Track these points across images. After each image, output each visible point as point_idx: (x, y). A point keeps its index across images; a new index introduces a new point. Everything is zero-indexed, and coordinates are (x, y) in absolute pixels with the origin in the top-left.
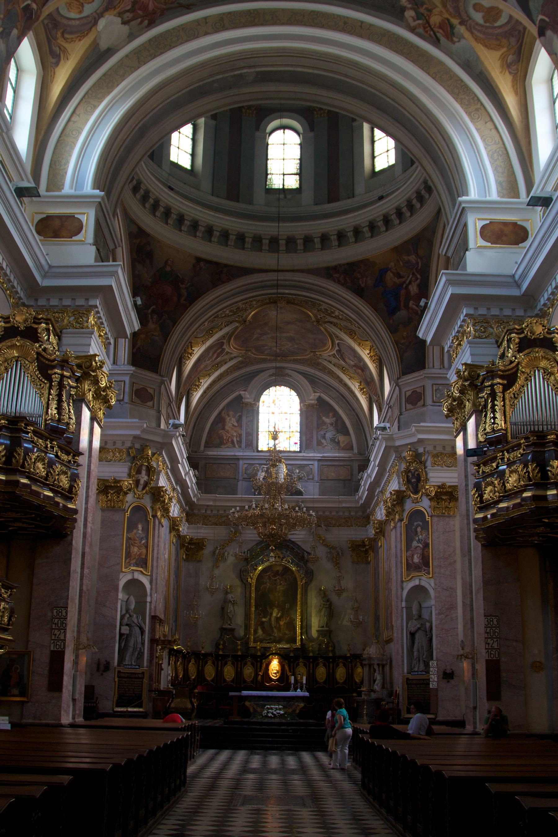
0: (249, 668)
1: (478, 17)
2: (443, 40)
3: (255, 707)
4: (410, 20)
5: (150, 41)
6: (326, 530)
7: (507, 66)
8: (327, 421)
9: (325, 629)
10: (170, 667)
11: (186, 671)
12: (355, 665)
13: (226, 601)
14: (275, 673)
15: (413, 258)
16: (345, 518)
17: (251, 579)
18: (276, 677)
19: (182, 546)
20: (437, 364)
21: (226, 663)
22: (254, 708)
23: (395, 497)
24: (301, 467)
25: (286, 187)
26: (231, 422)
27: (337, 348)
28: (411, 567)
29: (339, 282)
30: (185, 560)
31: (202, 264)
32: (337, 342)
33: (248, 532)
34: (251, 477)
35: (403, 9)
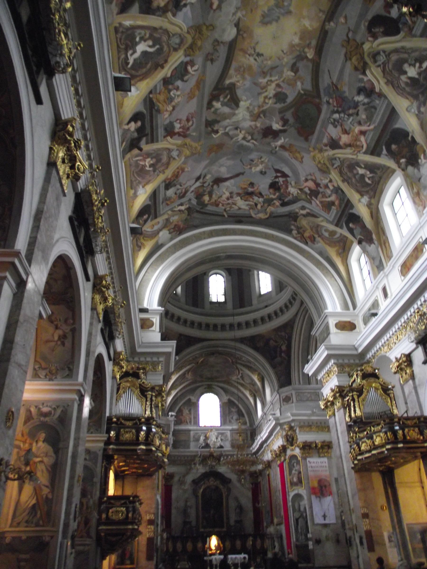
1: (326, 234)
2: (309, 243)
4: (295, 235)
5: (180, 241)
7: (339, 254)
8: (234, 410)
15: (283, 334)
20: (297, 382)
23: (281, 448)
24: (222, 434)
25: (219, 301)
26: (186, 411)
27: (241, 375)
28: (292, 484)
29: (247, 345)
31: (182, 337)
32: (241, 372)
34: (198, 440)
35: (292, 230)
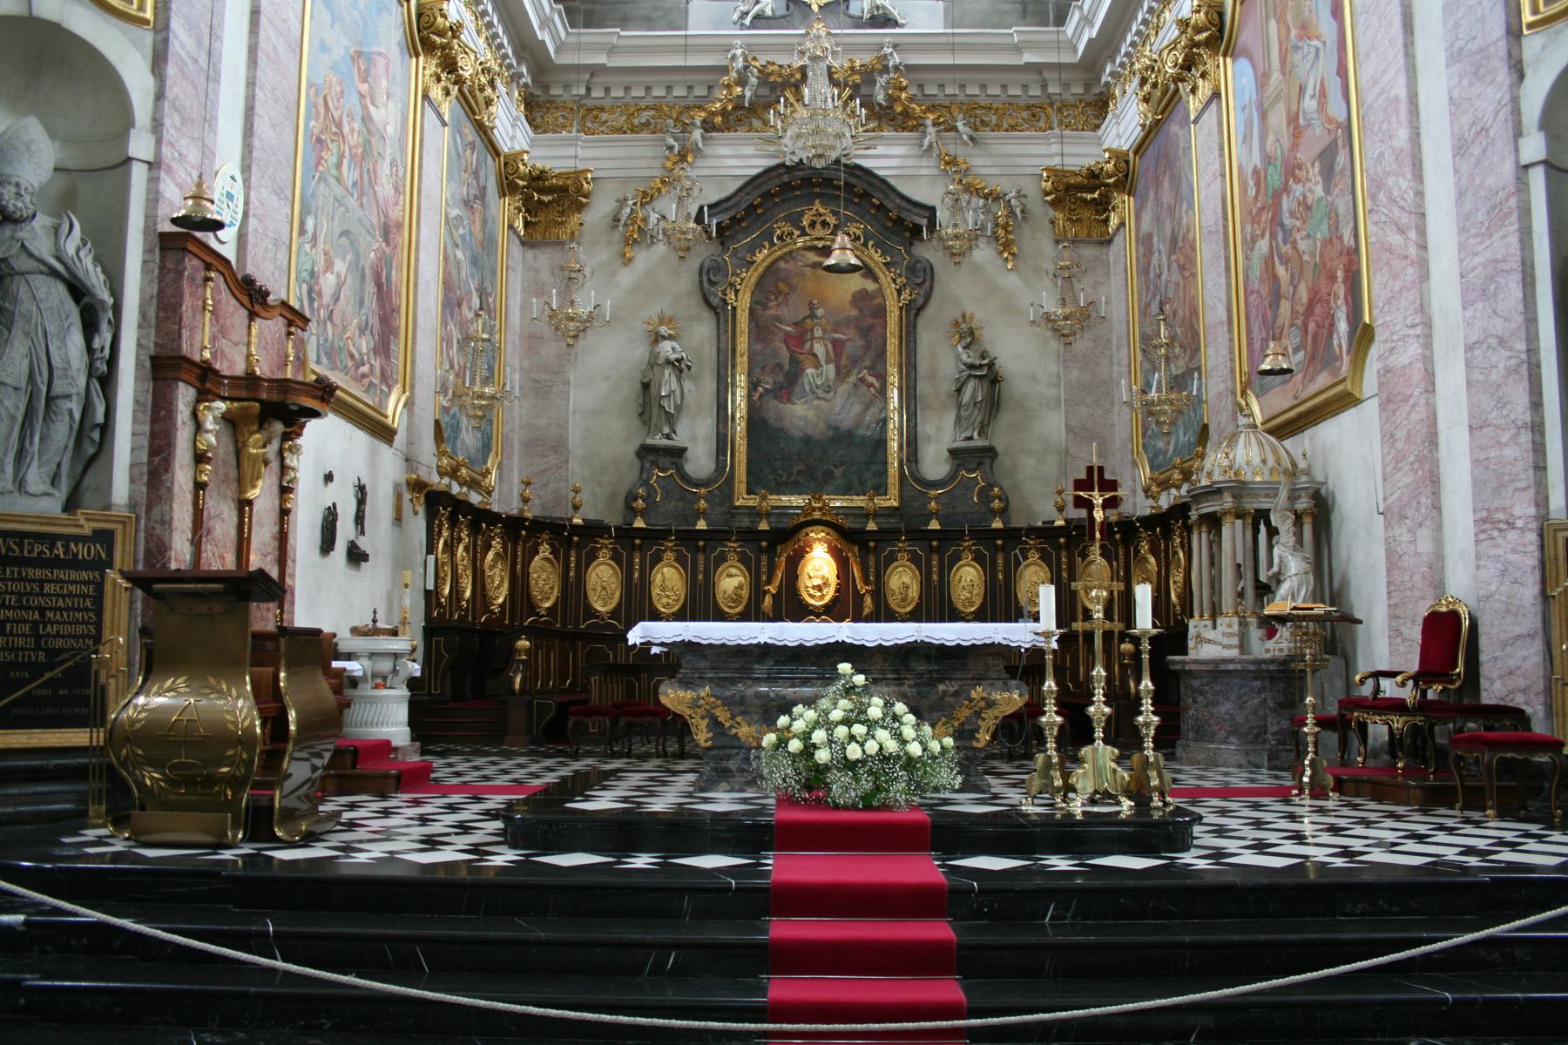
0: (733, 571)
3: (722, 715)
6: (971, 138)
9: (979, 442)
10: (431, 558)
11: (520, 584)
12: (1084, 555)
13: (653, 363)
14: (819, 588)
16: (1028, 107)
17: (737, 291)
18: (822, 597)
19: (507, 186)
21: (657, 559)
22: (715, 724)
30: (523, 243)
33: (724, 151)
